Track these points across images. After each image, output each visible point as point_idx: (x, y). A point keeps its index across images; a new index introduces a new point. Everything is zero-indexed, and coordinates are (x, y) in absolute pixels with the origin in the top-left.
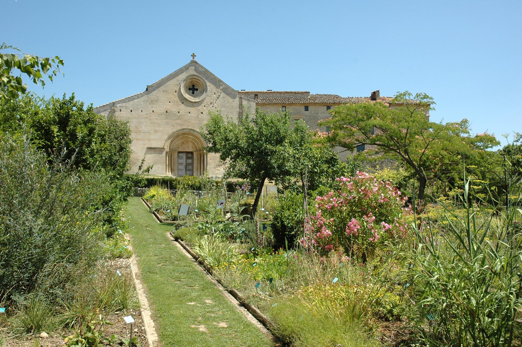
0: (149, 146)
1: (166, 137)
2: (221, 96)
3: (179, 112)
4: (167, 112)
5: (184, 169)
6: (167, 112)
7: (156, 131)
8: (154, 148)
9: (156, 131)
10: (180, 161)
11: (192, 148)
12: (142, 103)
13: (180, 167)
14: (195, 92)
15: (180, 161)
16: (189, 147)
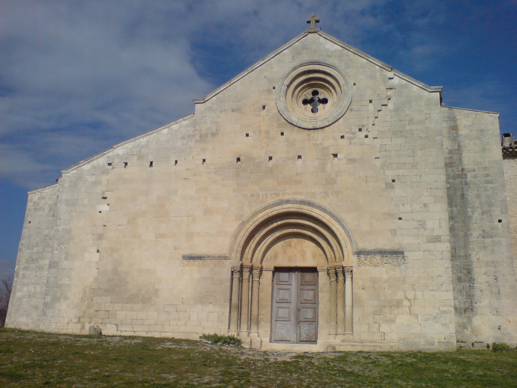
0: (187, 252)
1: (233, 227)
2: (391, 106)
3: (270, 158)
4: (238, 160)
5: (293, 318)
6: (238, 160)
7: (208, 212)
8: (200, 258)
9: (208, 212)
10: (282, 294)
11: (314, 256)
12: (179, 144)
13: (282, 313)
14: (320, 106)
15: (282, 294)
16: (303, 256)
